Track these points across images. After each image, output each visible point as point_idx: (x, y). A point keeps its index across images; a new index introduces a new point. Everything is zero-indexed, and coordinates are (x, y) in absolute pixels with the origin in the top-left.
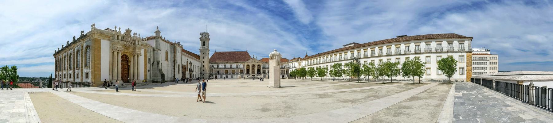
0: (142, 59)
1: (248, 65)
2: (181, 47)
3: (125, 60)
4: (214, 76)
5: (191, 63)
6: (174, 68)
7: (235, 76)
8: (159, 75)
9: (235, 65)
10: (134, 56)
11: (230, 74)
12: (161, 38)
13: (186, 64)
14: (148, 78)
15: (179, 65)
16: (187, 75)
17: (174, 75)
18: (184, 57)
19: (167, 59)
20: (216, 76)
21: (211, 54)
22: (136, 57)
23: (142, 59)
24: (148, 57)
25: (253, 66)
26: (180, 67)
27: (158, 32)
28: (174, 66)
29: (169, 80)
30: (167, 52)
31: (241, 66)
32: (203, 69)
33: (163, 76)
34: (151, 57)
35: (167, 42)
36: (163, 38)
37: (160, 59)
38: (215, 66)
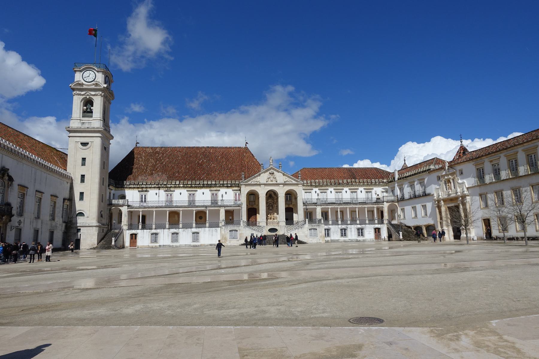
4: (127, 234)
9: (207, 191)
11: (187, 226)
20: (134, 237)
25: (272, 196)
31: (227, 196)
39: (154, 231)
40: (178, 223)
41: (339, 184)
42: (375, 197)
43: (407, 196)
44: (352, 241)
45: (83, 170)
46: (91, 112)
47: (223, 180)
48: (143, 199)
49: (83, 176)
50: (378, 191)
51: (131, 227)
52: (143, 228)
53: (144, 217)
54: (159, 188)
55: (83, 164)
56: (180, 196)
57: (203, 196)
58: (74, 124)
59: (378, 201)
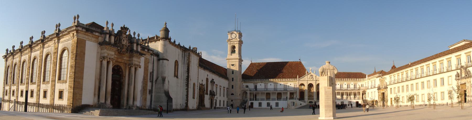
0: (141, 72)
2: (199, 55)
3: (118, 72)
5: (213, 82)
6: (187, 89)
7: (282, 104)
8: (164, 99)
13: (204, 83)
14: (148, 103)
15: (194, 84)
18: (202, 71)
19: (176, 76)
22: (133, 69)
23: (141, 72)
24: (150, 70)
26: (196, 88)
27: (167, 31)
28: (187, 85)
29: (179, 107)
30: (176, 62)
33: (170, 99)
34: (153, 70)
35: (179, 46)
36: (172, 41)
37: (166, 75)
39: (260, 101)
40: (270, 99)
45: (233, 76)
46: (235, 51)
47: (289, 78)
49: (233, 79)
51: (251, 100)
52: (256, 100)
53: (256, 95)
58: (229, 56)
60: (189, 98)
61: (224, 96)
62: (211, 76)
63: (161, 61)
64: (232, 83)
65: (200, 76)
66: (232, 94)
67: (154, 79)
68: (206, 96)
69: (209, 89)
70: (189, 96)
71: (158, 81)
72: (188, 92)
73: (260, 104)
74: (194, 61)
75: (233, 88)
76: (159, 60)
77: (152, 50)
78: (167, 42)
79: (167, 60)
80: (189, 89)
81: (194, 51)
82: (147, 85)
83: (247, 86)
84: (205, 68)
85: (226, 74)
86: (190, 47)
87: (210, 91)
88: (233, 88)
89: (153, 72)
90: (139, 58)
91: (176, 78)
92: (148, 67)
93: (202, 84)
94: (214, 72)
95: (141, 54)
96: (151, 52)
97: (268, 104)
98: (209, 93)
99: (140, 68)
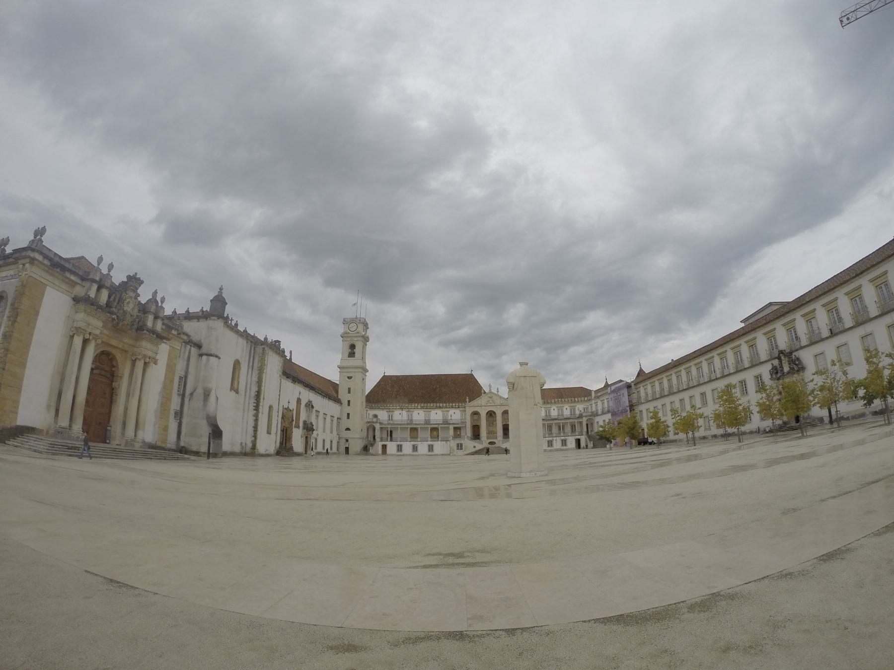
0: (157, 374)
1: (476, 413)
2: (281, 353)
4: (379, 444)
5: (310, 406)
6: (256, 416)
9: (439, 411)
10: (134, 362)
12: (226, 320)
13: (293, 406)
15: (271, 407)
16: (297, 443)
17: (255, 436)
18: (288, 385)
19: (234, 388)
21: (372, 381)
25: (491, 414)
26: (275, 414)
27: (219, 302)
28: (257, 408)
29: (237, 449)
30: (237, 364)
31: (455, 415)
32: (345, 423)
33: (216, 433)
35: (245, 335)
38: (383, 415)
39: (399, 443)
41: (548, 403)
42: (577, 413)
43: (600, 413)
44: (557, 450)
47: (452, 402)
48: (390, 418)
49: (349, 401)
50: (580, 407)
52: (391, 440)
53: (391, 432)
54: (402, 409)
55: (349, 392)
56: (419, 415)
57: (436, 415)
59: (581, 416)
60: (259, 433)
61: (332, 432)
62: (307, 395)
63: (204, 358)
64: (348, 410)
65: (283, 395)
66: (348, 429)
67: (188, 392)
68: (295, 430)
69: (303, 417)
70: (259, 428)
71: (195, 394)
72: (256, 420)
73: (400, 448)
74: (273, 364)
75: (348, 418)
76: (201, 355)
77: (187, 335)
78: (219, 324)
79: (217, 356)
80: (260, 415)
81: (275, 346)
82: (169, 399)
83: (376, 416)
84: (296, 380)
85: (337, 392)
86: (266, 339)
87: (305, 422)
88: (348, 418)
89: (186, 377)
90: (157, 345)
91: (233, 393)
92: (175, 364)
93: (288, 409)
94: (312, 388)
95: (160, 337)
96: (185, 338)
97: (415, 448)
98: (301, 425)
99: (155, 363)
